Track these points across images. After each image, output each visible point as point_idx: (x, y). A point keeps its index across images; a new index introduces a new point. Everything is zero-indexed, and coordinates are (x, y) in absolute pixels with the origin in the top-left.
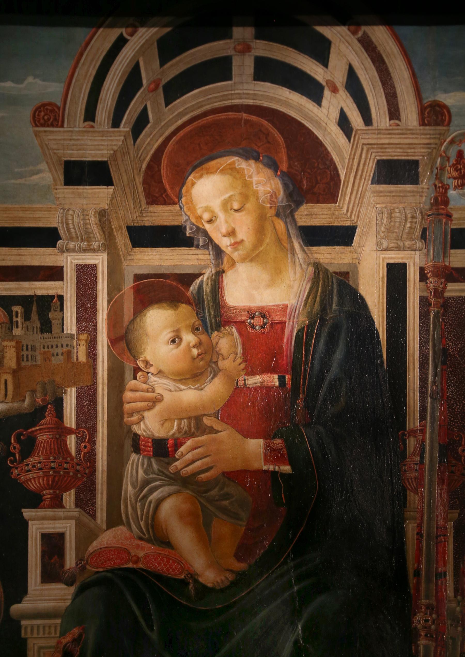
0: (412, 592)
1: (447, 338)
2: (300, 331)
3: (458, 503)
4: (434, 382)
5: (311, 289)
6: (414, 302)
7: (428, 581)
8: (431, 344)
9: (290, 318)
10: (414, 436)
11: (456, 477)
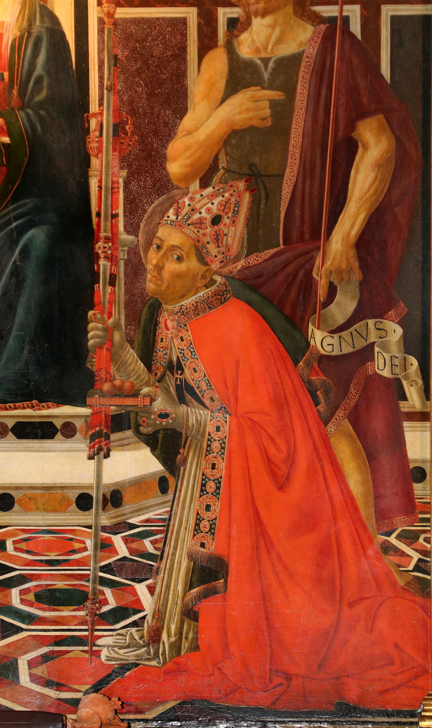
0: (95, 227)
1: (117, 47)
2: (14, 41)
3: (126, 165)
4: (109, 79)
5: (21, 10)
6: (93, 21)
7: (106, 219)
8: (106, 51)
9: (6, 31)
10: (96, 118)
11: (124, 147)
